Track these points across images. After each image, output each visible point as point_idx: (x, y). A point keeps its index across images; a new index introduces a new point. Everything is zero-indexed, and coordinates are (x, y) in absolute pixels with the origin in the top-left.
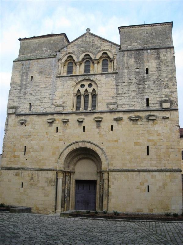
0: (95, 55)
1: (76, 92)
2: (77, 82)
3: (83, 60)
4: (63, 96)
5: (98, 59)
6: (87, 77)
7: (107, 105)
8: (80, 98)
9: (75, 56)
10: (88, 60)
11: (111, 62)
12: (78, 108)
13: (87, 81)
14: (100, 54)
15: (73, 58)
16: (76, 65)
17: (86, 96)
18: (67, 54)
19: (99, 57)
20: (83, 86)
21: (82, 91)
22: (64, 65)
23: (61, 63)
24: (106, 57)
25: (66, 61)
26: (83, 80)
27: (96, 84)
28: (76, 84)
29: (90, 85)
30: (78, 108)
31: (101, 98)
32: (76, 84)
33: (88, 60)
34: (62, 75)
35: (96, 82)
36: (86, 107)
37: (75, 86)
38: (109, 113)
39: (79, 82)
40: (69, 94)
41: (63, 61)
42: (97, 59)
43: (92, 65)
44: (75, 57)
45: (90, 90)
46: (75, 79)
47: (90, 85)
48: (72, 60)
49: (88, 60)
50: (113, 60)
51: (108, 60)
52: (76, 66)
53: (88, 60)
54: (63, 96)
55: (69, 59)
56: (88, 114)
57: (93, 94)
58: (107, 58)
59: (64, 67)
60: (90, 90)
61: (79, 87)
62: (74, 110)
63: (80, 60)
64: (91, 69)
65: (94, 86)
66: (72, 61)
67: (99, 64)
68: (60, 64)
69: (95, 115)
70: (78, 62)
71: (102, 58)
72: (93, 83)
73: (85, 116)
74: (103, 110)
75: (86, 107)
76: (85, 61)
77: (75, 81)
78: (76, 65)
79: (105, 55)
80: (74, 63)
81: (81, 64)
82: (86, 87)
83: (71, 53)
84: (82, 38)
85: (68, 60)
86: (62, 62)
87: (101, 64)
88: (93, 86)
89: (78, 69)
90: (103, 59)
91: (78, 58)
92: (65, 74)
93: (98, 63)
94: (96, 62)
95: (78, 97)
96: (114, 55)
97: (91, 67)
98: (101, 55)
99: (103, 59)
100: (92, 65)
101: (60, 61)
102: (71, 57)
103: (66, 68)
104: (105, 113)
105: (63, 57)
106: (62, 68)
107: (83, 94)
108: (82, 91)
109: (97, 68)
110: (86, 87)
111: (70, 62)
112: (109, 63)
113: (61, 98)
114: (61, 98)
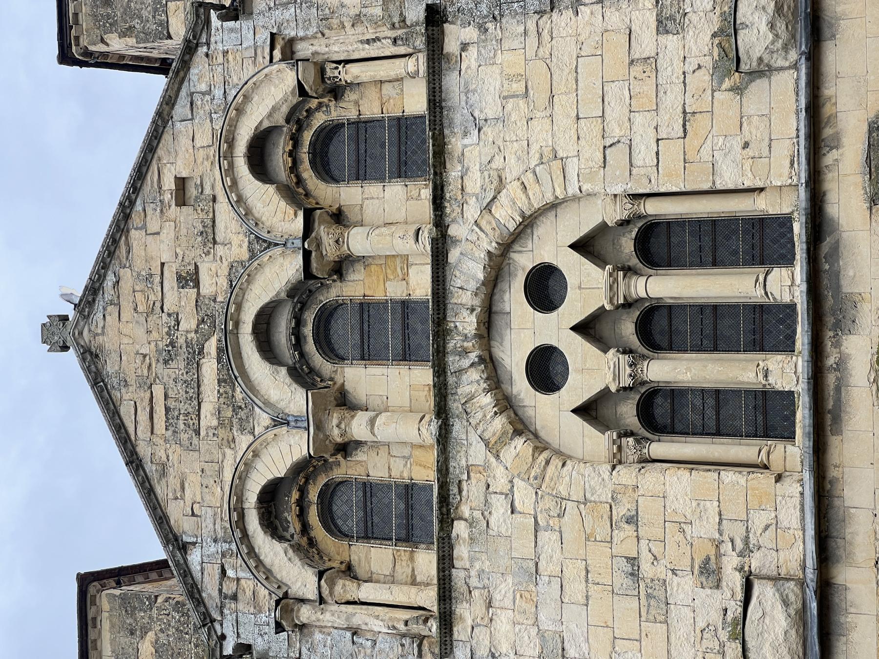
0: (262, 243)
1: (594, 441)
2: (499, 424)
3: (303, 375)
4: (635, 575)
5: (301, 214)
6: (465, 323)
7: (738, 90)
8: (675, 395)
9: (265, 457)
10: (308, 331)
11: (336, 91)
12: (765, 415)
13: (499, 321)
14: (264, 199)
15: (280, 470)
16: (346, 448)
17: (659, 327)
18: (245, 535)
19: (290, 211)
20: (546, 369)
21: (592, 370)
22: (349, 571)
23: (322, 600)
24: (296, 140)
25: (307, 549)
26: (490, 363)
27: (528, 224)
28: (518, 433)
29: (544, 288)
30: (765, 415)
31: (672, 152)
32: (519, 442)
33: (317, 327)
34: (429, 598)
35: (507, 215)
36: (762, 328)
37: (540, 445)
38: (837, 58)
39: (506, 404)
40: (620, 511)
41: (301, 579)
42: (299, 223)
43: (355, 287)
44: (273, 450)
45: (588, 287)
46: (471, 451)
47: (544, 288)
48: (303, 491)
49: (317, 327)
50: (322, 71)
51: (319, 120)
52: (359, 444)
53: (308, 331)
54: (635, 575)
55: (294, 526)
56: (838, 287)
57: (634, 261)
58: (307, 137)
59: (361, 572)
60: (588, 287)
61: (552, 412)
62: (794, 453)
63: (294, 399)
64: (395, 291)
65: (551, 246)
66: (313, 494)
67: (352, 215)
68: (333, 616)
69: (847, 197)
70: (319, 427)
71: (300, 181)
72: (524, 261)
73: (845, 324)
74: (790, 125)
75: (762, 328)
76: (318, 360)
77: (494, 448)
78: (346, 448)
79: (279, 158)
80: (337, 474)
81: (345, 401)
82: (554, 329)
83: (240, 499)
84: (116, 394)
85: (305, 529)
86: (311, 593)
87: (348, 194)
88: (548, 259)
89: (388, 429)
90: (307, 173)
91: (281, 421)
92: (426, 561)
93: (338, 217)
94: (325, 233)
95: (661, 412)
96: (277, 54)
97: (379, 296)
98: (270, 189)
99: (307, 173)
100: (355, 287)
101: (305, 614)
102: (271, 494)
103: (376, 557)
104: (828, 90)
105: (269, 575)
106: (367, 592)
107: (625, 359)
108: (592, 370)
109: (385, 216)
110: (554, 329)
111: (314, 505)
112: (344, 111)
113: (655, 601)
114: (655, 601)
